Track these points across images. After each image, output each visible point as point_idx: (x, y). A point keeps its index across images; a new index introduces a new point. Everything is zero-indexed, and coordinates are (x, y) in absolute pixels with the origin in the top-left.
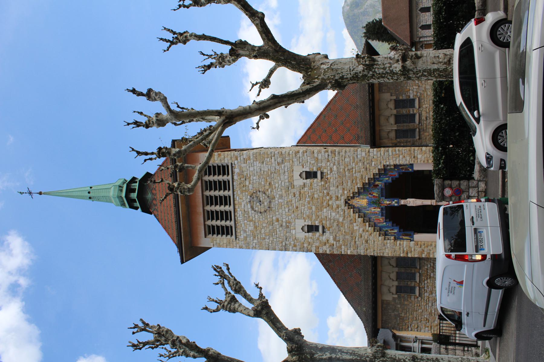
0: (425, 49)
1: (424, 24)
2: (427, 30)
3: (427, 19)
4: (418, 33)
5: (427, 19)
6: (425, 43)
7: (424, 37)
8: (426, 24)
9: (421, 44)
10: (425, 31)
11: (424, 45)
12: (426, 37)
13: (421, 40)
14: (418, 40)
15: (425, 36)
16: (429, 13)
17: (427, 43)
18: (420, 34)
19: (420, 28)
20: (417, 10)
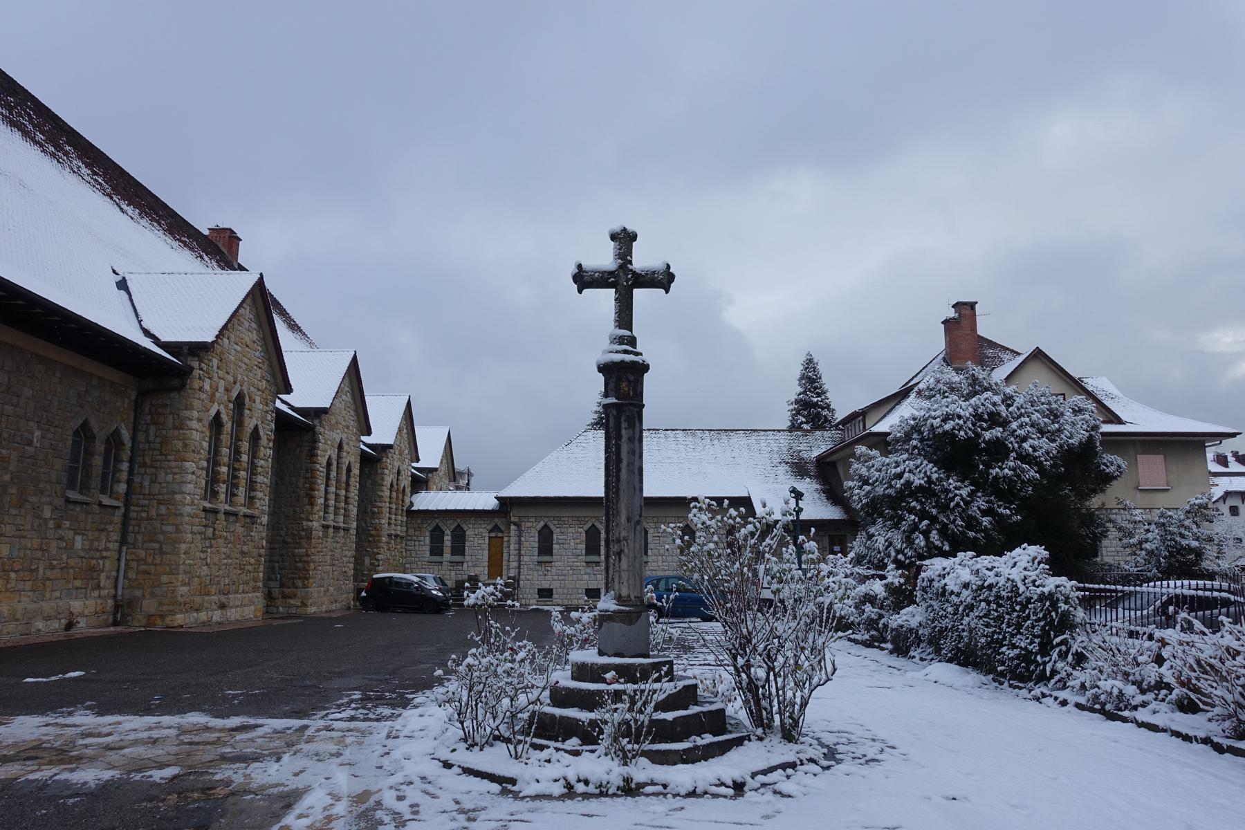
0: (490, 537)
1: (555, 536)
2: (536, 545)
3: (566, 546)
4: (533, 520)
5: (566, 546)
6: (505, 539)
7: (520, 537)
8: (555, 542)
9: (503, 528)
10: (537, 539)
11: (500, 535)
12: (520, 543)
13: (513, 527)
14: (512, 519)
15: (523, 539)
16: (584, 552)
17: (505, 544)
18: (530, 524)
19: (546, 526)
20: (594, 520)
